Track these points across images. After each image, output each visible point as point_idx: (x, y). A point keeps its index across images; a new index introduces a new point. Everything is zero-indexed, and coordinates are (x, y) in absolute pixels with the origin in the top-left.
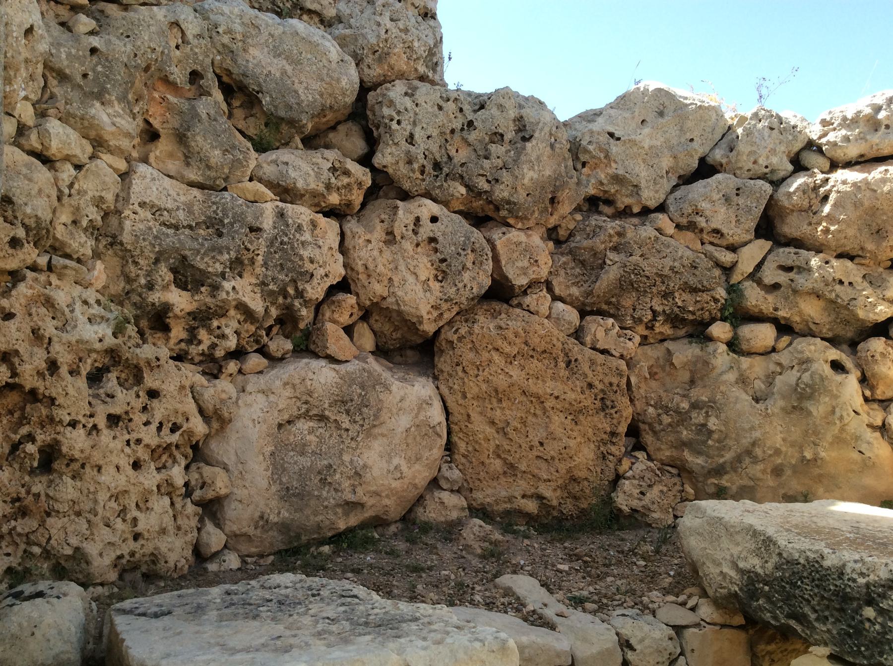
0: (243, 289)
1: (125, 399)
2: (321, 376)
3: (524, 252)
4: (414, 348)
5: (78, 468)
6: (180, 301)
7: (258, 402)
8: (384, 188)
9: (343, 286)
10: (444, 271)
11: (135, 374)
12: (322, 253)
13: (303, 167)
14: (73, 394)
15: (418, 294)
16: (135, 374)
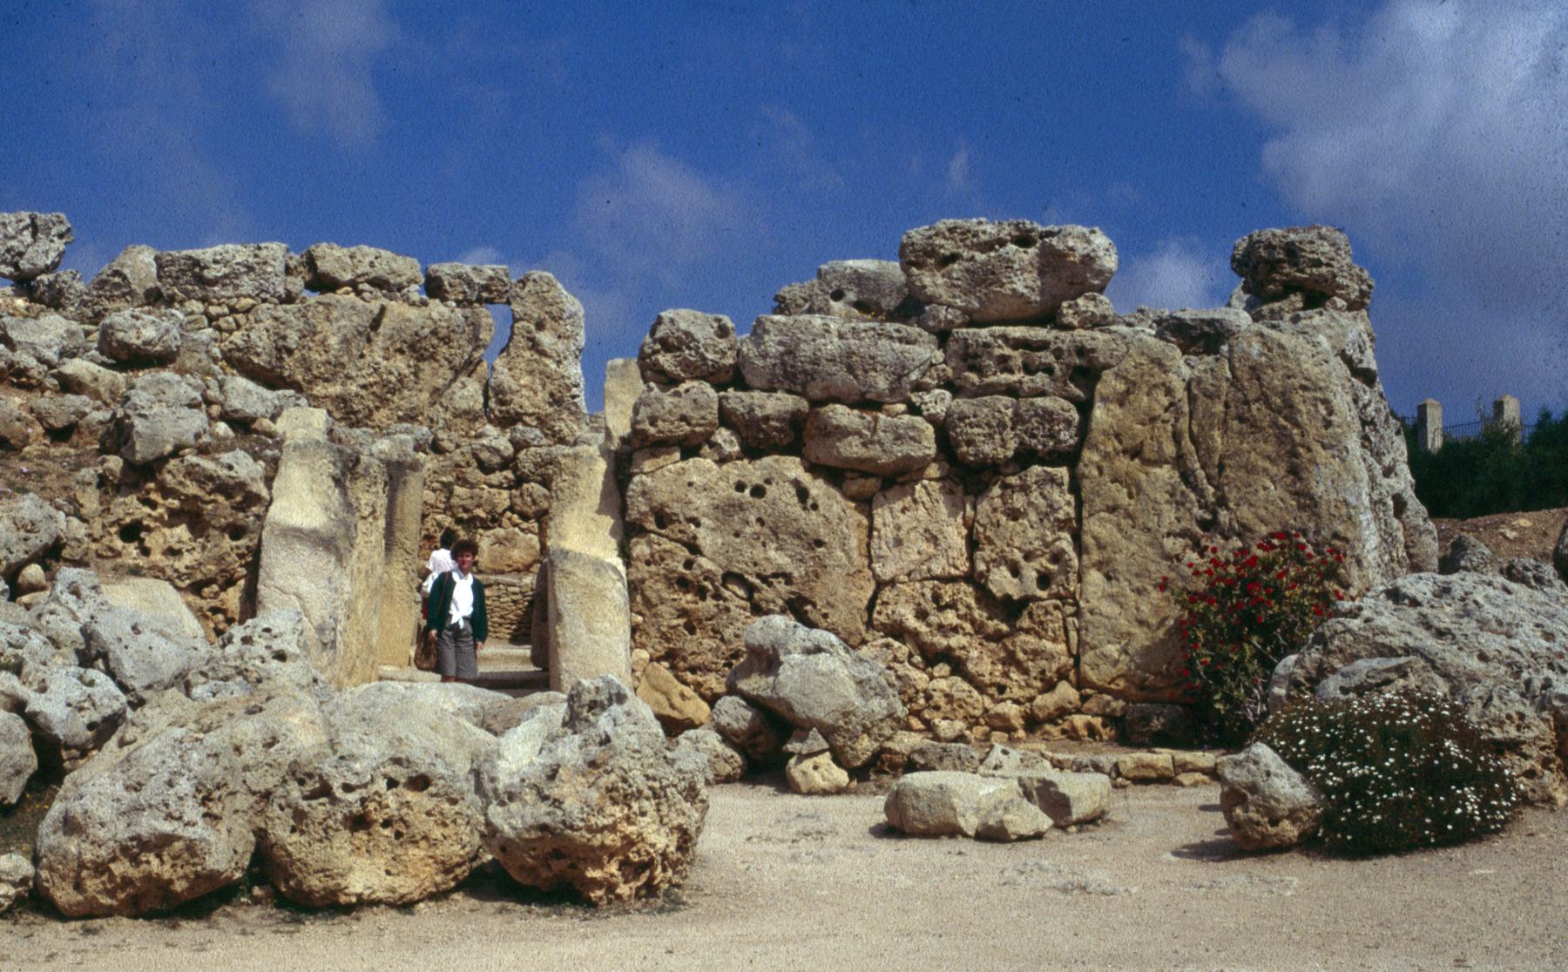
0: (480, 513)
6: (465, 516)
10: (534, 502)
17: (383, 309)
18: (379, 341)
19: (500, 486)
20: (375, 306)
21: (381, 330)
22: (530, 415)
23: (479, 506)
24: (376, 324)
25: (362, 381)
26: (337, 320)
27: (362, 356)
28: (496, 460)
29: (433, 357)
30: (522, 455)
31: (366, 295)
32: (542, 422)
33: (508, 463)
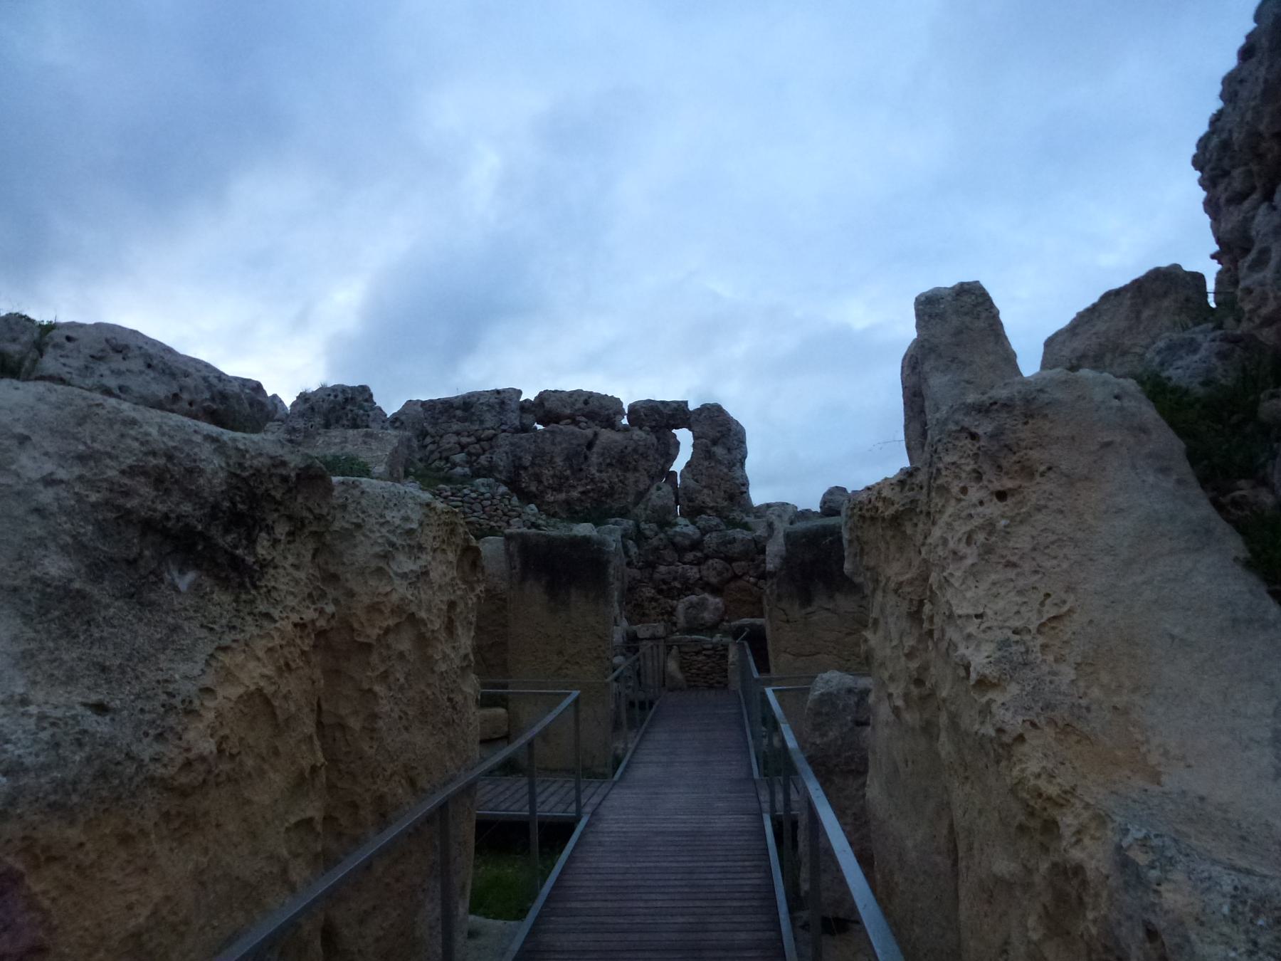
0: (677, 584)
1: (654, 604)
2: (694, 598)
3: (738, 566)
4: (716, 590)
5: (647, 615)
6: (664, 587)
7: (681, 605)
8: (707, 557)
9: (701, 579)
10: (720, 574)
11: (656, 600)
12: (693, 572)
13: (690, 556)
14: (646, 604)
15: (714, 580)
16: (656, 600)
17: (596, 434)
18: (594, 459)
19: (691, 563)
20: (589, 432)
21: (595, 449)
22: (711, 508)
23: (675, 579)
24: (590, 445)
25: (581, 489)
26: (560, 443)
27: (581, 470)
28: (687, 542)
29: (636, 469)
30: (707, 538)
31: (583, 425)
32: (718, 512)
33: (696, 545)
